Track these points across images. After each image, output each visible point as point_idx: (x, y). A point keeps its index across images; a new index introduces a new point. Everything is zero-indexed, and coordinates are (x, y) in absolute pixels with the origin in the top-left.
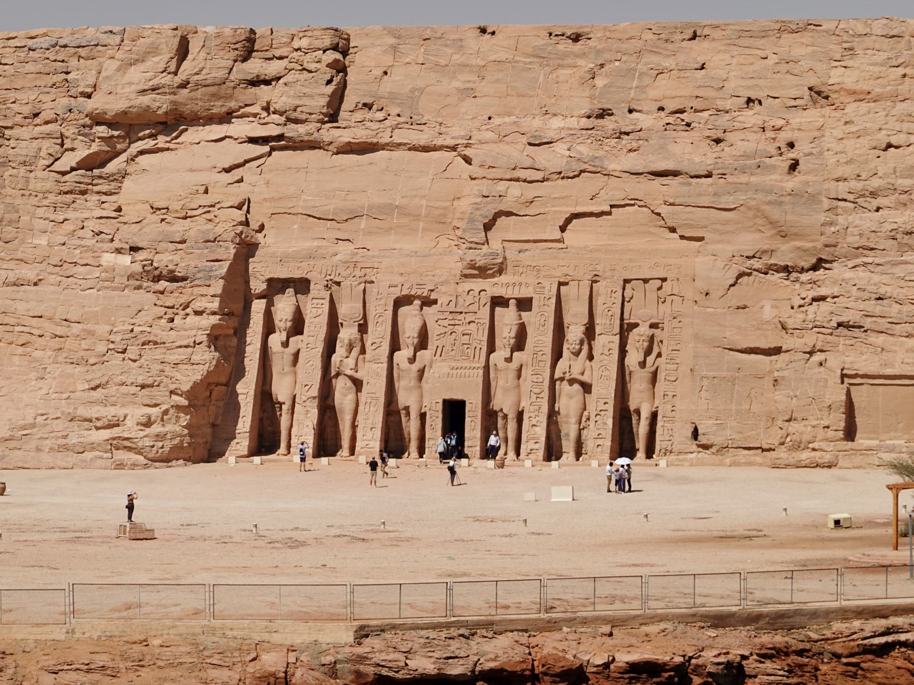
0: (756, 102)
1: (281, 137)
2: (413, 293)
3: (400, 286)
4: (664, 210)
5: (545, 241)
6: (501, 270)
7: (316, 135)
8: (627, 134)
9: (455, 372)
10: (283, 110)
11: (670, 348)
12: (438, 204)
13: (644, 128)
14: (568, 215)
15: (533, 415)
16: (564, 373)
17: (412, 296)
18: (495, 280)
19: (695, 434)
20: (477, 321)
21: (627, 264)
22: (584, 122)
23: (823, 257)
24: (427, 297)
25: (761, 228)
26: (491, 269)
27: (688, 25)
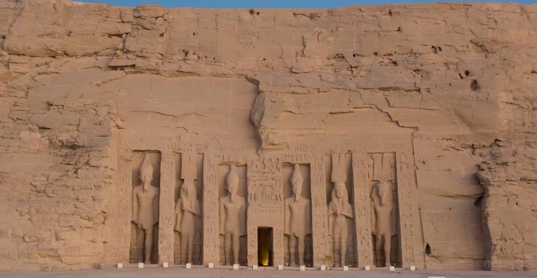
0: (438, 49)
1: (133, 66)
2: (231, 160)
8: (356, 67)
10: (134, 50)
16: (337, 211)
17: (230, 162)
18: (283, 152)
19: (428, 249)
23: (499, 139)
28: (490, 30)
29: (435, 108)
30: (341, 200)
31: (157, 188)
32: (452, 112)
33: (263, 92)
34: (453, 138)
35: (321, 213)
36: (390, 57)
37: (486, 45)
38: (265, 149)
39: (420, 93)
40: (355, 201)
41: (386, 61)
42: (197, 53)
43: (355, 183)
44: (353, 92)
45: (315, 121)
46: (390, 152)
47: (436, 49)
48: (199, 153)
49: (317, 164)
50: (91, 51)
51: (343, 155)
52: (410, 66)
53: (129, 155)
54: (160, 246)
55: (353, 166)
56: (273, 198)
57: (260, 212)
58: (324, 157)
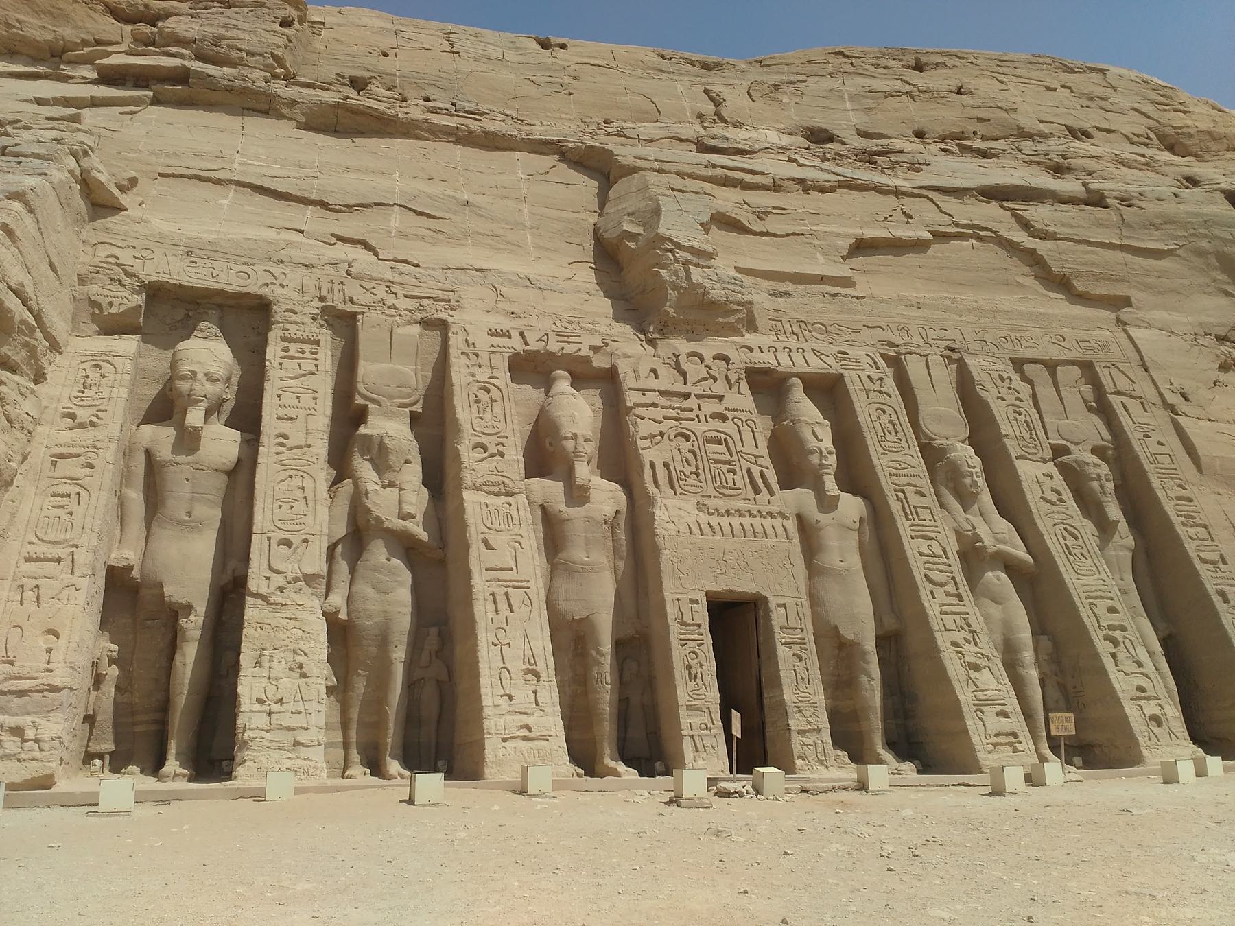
1: (181, 77)
2: (554, 346)
3: (515, 334)
4: (1042, 247)
5: (822, 279)
6: (751, 324)
7: (262, 84)
9: (725, 521)
12: (553, 213)
15: (959, 636)
20: (730, 415)
21: (1004, 334)
22: (786, 140)
24: (587, 360)
26: (733, 312)
27: (903, 52)
31: (249, 436)
36: (964, 142)
37: (1187, 142)
40: (1032, 506)
41: (956, 149)
42: (399, 90)
43: (1013, 449)
44: (907, 199)
46: (1073, 363)
48: (426, 323)
49: (865, 379)
50: (37, 29)
51: (935, 359)
53: (129, 300)
54: (249, 686)
55: (983, 394)
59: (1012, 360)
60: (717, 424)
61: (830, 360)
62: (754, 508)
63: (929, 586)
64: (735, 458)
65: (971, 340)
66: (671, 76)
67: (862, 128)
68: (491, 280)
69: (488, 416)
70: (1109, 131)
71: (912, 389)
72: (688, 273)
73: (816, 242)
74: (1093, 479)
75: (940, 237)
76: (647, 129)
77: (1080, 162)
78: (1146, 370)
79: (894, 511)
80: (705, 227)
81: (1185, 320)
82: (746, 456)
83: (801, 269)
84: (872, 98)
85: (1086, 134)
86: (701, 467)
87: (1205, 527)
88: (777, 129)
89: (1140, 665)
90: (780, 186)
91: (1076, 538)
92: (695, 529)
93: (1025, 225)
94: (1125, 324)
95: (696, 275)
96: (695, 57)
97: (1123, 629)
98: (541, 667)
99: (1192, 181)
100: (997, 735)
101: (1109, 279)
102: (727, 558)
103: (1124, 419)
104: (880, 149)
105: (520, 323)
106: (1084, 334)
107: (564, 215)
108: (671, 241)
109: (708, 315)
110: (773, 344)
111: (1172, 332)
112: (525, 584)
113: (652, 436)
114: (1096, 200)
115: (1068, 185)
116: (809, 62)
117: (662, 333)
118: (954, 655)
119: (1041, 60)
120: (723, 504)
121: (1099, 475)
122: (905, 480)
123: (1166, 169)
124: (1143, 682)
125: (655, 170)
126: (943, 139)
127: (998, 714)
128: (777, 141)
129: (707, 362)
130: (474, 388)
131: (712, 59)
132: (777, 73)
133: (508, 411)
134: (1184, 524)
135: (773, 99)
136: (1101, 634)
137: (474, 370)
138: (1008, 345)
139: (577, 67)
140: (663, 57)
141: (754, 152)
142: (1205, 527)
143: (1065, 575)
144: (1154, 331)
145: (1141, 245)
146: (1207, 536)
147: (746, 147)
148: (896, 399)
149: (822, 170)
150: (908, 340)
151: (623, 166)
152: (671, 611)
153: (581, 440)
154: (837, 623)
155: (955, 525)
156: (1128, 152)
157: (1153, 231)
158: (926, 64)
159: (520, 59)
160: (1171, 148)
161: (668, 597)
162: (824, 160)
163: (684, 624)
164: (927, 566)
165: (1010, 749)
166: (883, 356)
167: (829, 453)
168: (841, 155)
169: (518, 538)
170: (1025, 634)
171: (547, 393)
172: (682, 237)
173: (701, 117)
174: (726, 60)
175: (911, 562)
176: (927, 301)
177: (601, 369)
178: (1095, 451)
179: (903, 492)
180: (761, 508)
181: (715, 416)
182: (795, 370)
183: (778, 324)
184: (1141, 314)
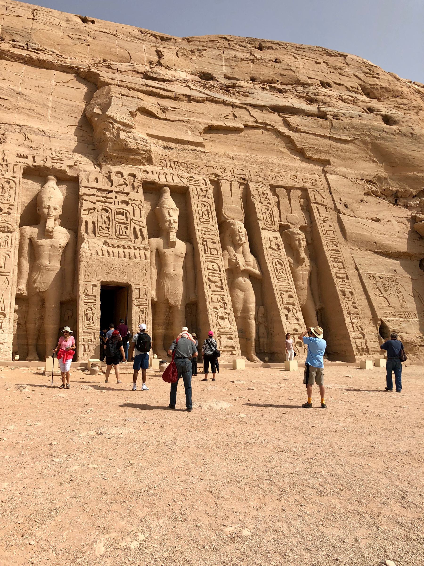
2: (49, 164)
3: (30, 158)
5: (189, 143)
6: (150, 161)
9: (116, 250)
11: (330, 248)
13: (244, 86)
14: (207, 126)
15: (217, 305)
17: (47, 168)
18: (143, 167)
20: (130, 202)
21: (269, 173)
22: (189, 77)
24: (64, 172)
25: (375, 159)
26: (141, 154)
27: (254, 40)
28: (376, 79)
29: (350, 139)
30: (240, 249)
32: (370, 146)
33: (107, 84)
34: (374, 180)
35: (215, 265)
37: (375, 92)
38: (112, 157)
39: (326, 119)
40: (265, 250)
41: (268, 88)
43: (261, 224)
44: (237, 109)
45: (190, 133)
47: (326, 85)
52: (301, 94)
55: (253, 200)
56: (128, 234)
57: (106, 253)
58: (209, 183)
59: (270, 185)
60: (124, 206)
61: (185, 180)
62: (131, 244)
63: (208, 283)
64: (129, 222)
65: (253, 176)
66: (142, 42)
67: (227, 74)
68: (24, 130)
69: (7, 194)
70: (340, 85)
71: (222, 196)
72: (118, 134)
73: (189, 125)
74: (296, 240)
75: (248, 127)
76: (123, 66)
77: (322, 97)
78: (331, 193)
79: (200, 250)
80: (133, 114)
81: (353, 172)
82: (134, 221)
83: (179, 137)
84: (235, 61)
85: (329, 85)
86: (111, 225)
87: (342, 263)
88: (186, 72)
89: (298, 320)
90: (178, 98)
91: (282, 265)
92: (100, 253)
93: (287, 125)
94: (326, 172)
95: (122, 135)
96: (158, 34)
97: (294, 304)
98: (7, 312)
99: (371, 110)
100: (225, 347)
101: (322, 152)
102: (114, 267)
103: (316, 215)
104: (232, 85)
105: (33, 152)
106: (306, 176)
107: (71, 103)
108: (112, 118)
109: (128, 155)
110: (159, 171)
111: (346, 177)
112: (7, 274)
113: (90, 209)
114: (323, 115)
115: (313, 108)
116: (210, 41)
117: (104, 161)
118: (213, 313)
119: (317, 49)
120: (116, 242)
121: (299, 238)
122: (208, 236)
123: (361, 104)
124: (297, 327)
125: (117, 85)
126: (263, 83)
127: (228, 338)
128: (185, 77)
129: (124, 177)
130: (3, 182)
131: (165, 35)
132: (194, 45)
133: (17, 193)
134: (332, 261)
135: (187, 57)
136: (283, 306)
137: (4, 173)
138: (270, 179)
139: (95, 32)
140: (142, 32)
141: (171, 81)
142: (342, 263)
143: (273, 281)
144: (338, 176)
145: (339, 137)
146: (342, 267)
147: (168, 79)
148: (212, 201)
149: (201, 92)
150: (225, 174)
151: (102, 82)
152: (81, 289)
153: (52, 209)
154: (168, 297)
155: (229, 257)
156: (345, 95)
157: (345, 131)
158: (264, 47)
159: (68, 25)
160: (368, 95)
161: (81, 283)
162: (205, 87)
163: (87, 295)
164: (210, 274)
165: (230, 353)
166: (211, 181)
167: (175, 222)
168: (213, 86)
169: (8, 252)
170: (252, 305)
171: (42, 186)
172: (118, 117)
173: (151, 62)
174: (173, 37)
175: (203, 272)
176: (237, 157)
177: (72, 176)
178: (302, 228)
179: (206, 241)
180: (135, 245)
181: (123, 202)
182: (166, 183)
183: (164, 162)
184: (333, 168)
